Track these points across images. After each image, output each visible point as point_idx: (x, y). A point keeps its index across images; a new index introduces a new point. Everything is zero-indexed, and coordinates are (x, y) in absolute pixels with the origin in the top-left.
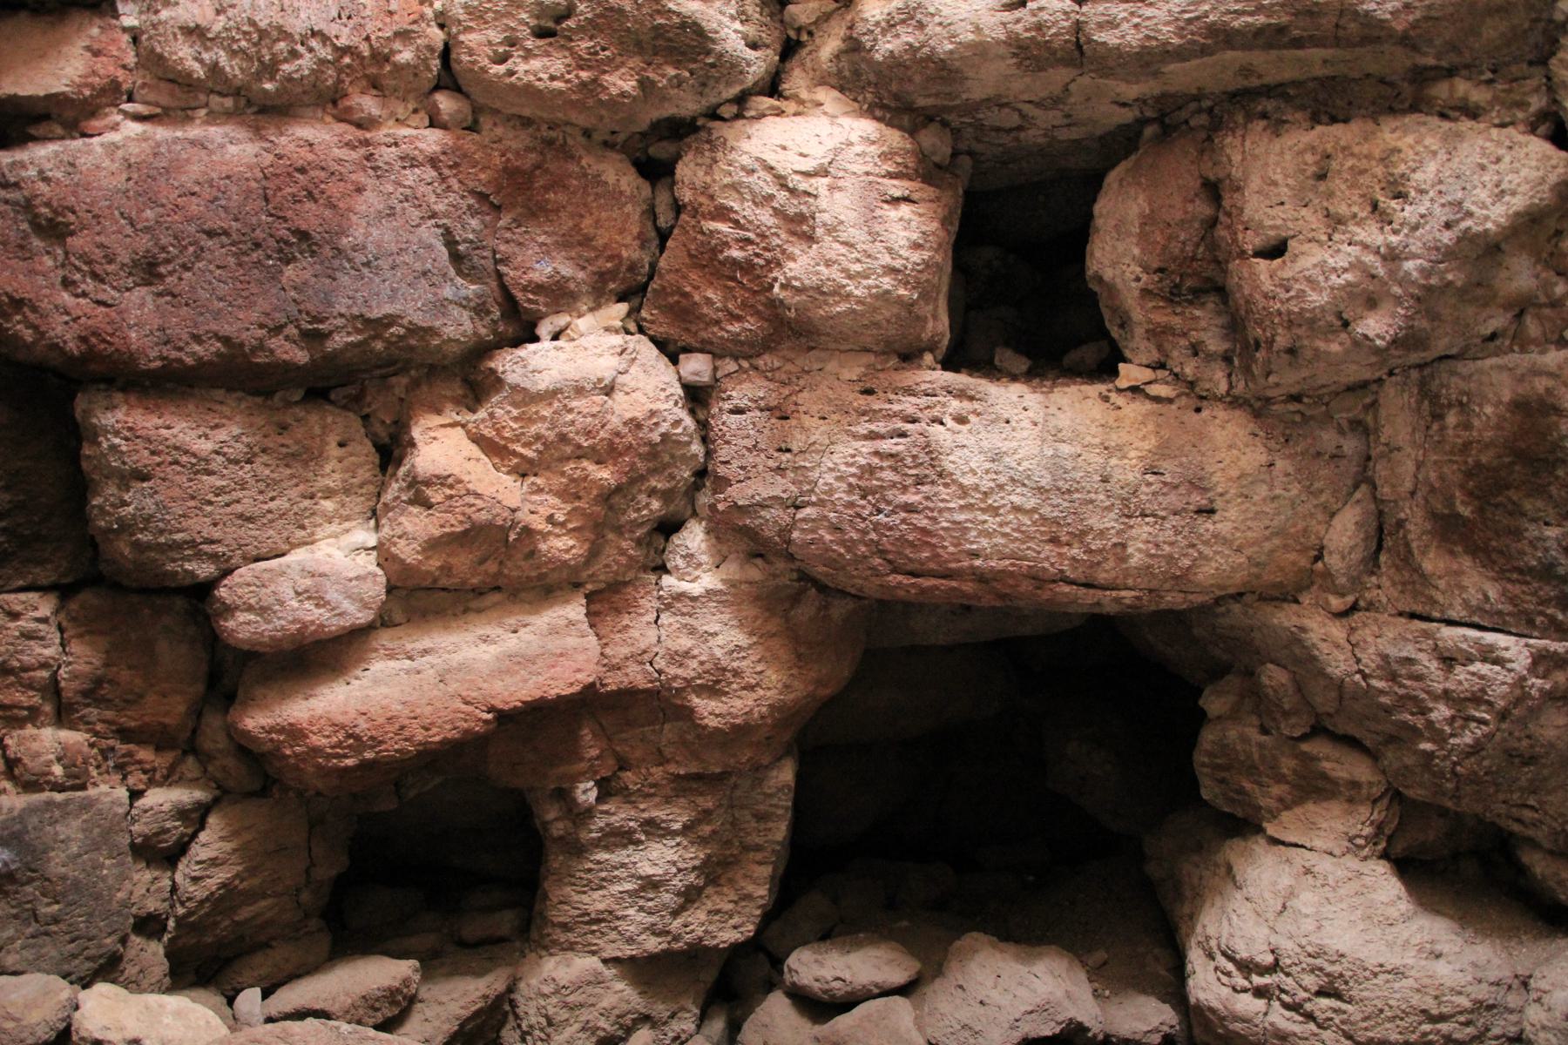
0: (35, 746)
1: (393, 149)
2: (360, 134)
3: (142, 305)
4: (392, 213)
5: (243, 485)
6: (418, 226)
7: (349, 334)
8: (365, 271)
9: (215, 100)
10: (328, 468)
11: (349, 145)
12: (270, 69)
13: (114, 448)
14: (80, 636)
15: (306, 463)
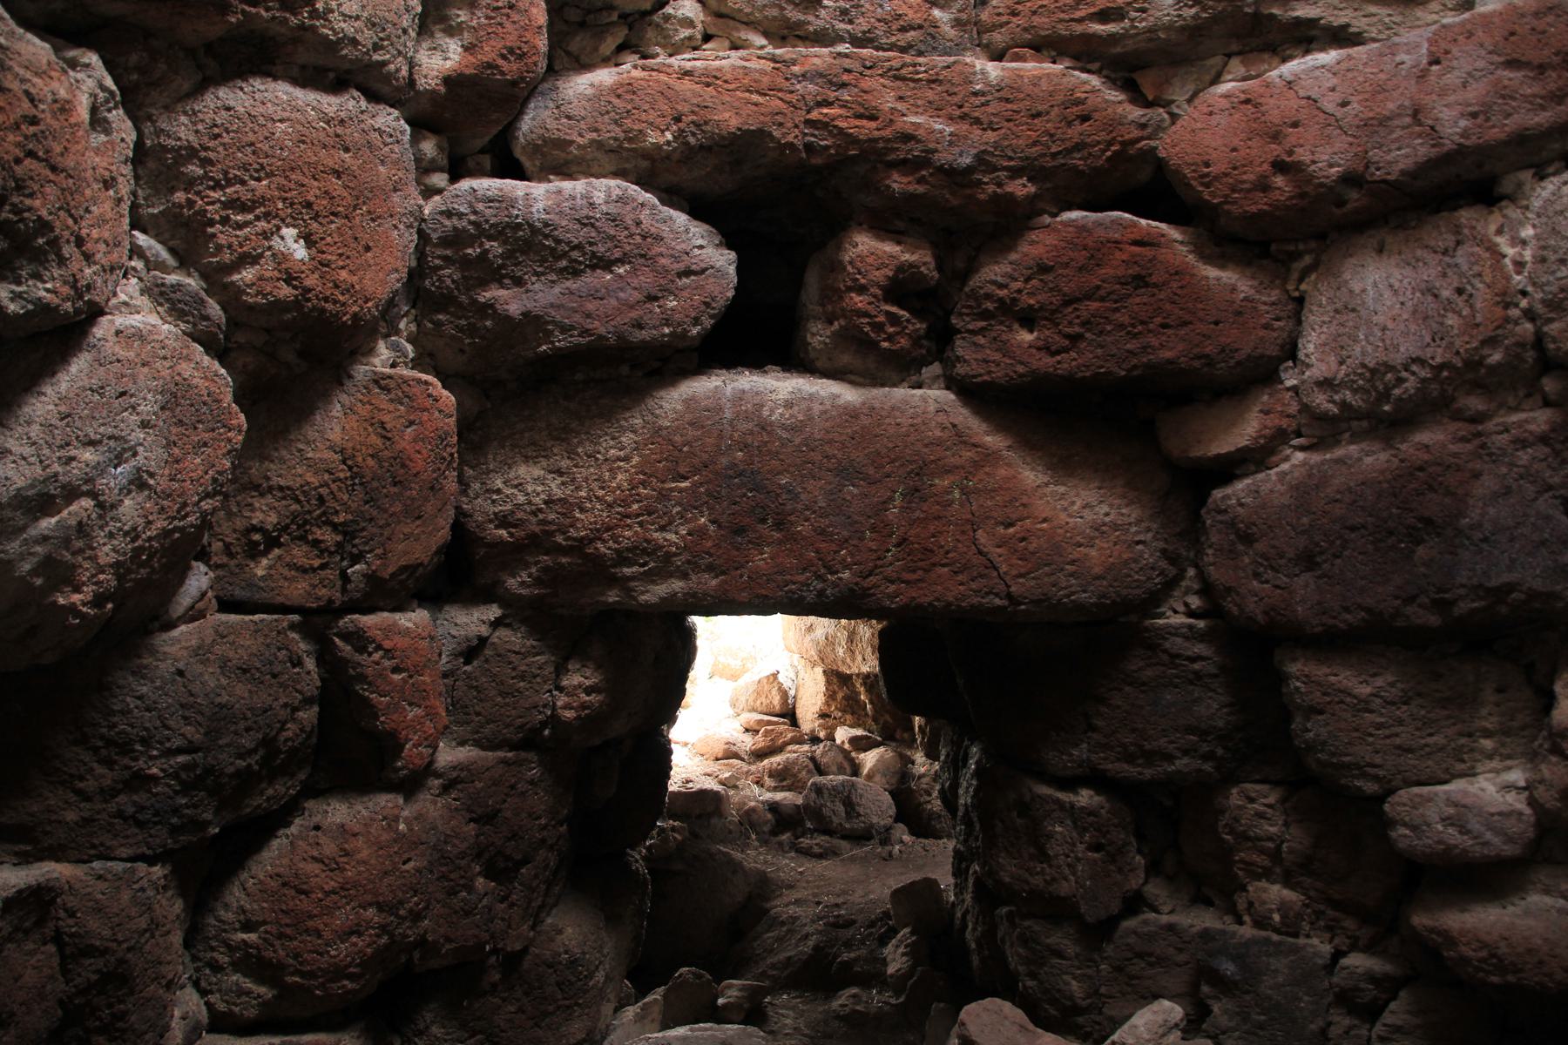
0: (1264, 896)
1: (1505, 436)
2: (1472, 428)
3: (1307, 586)
4: (1508, 491)
5: (1401, 722)
6: (1536, 499)
7: (1473, 601)
8: (1485, 546)
9: (1355, 424)
10: (1484, 712)
11: (1463, 439)
12: (1385, 396)
13: (1297, 689)
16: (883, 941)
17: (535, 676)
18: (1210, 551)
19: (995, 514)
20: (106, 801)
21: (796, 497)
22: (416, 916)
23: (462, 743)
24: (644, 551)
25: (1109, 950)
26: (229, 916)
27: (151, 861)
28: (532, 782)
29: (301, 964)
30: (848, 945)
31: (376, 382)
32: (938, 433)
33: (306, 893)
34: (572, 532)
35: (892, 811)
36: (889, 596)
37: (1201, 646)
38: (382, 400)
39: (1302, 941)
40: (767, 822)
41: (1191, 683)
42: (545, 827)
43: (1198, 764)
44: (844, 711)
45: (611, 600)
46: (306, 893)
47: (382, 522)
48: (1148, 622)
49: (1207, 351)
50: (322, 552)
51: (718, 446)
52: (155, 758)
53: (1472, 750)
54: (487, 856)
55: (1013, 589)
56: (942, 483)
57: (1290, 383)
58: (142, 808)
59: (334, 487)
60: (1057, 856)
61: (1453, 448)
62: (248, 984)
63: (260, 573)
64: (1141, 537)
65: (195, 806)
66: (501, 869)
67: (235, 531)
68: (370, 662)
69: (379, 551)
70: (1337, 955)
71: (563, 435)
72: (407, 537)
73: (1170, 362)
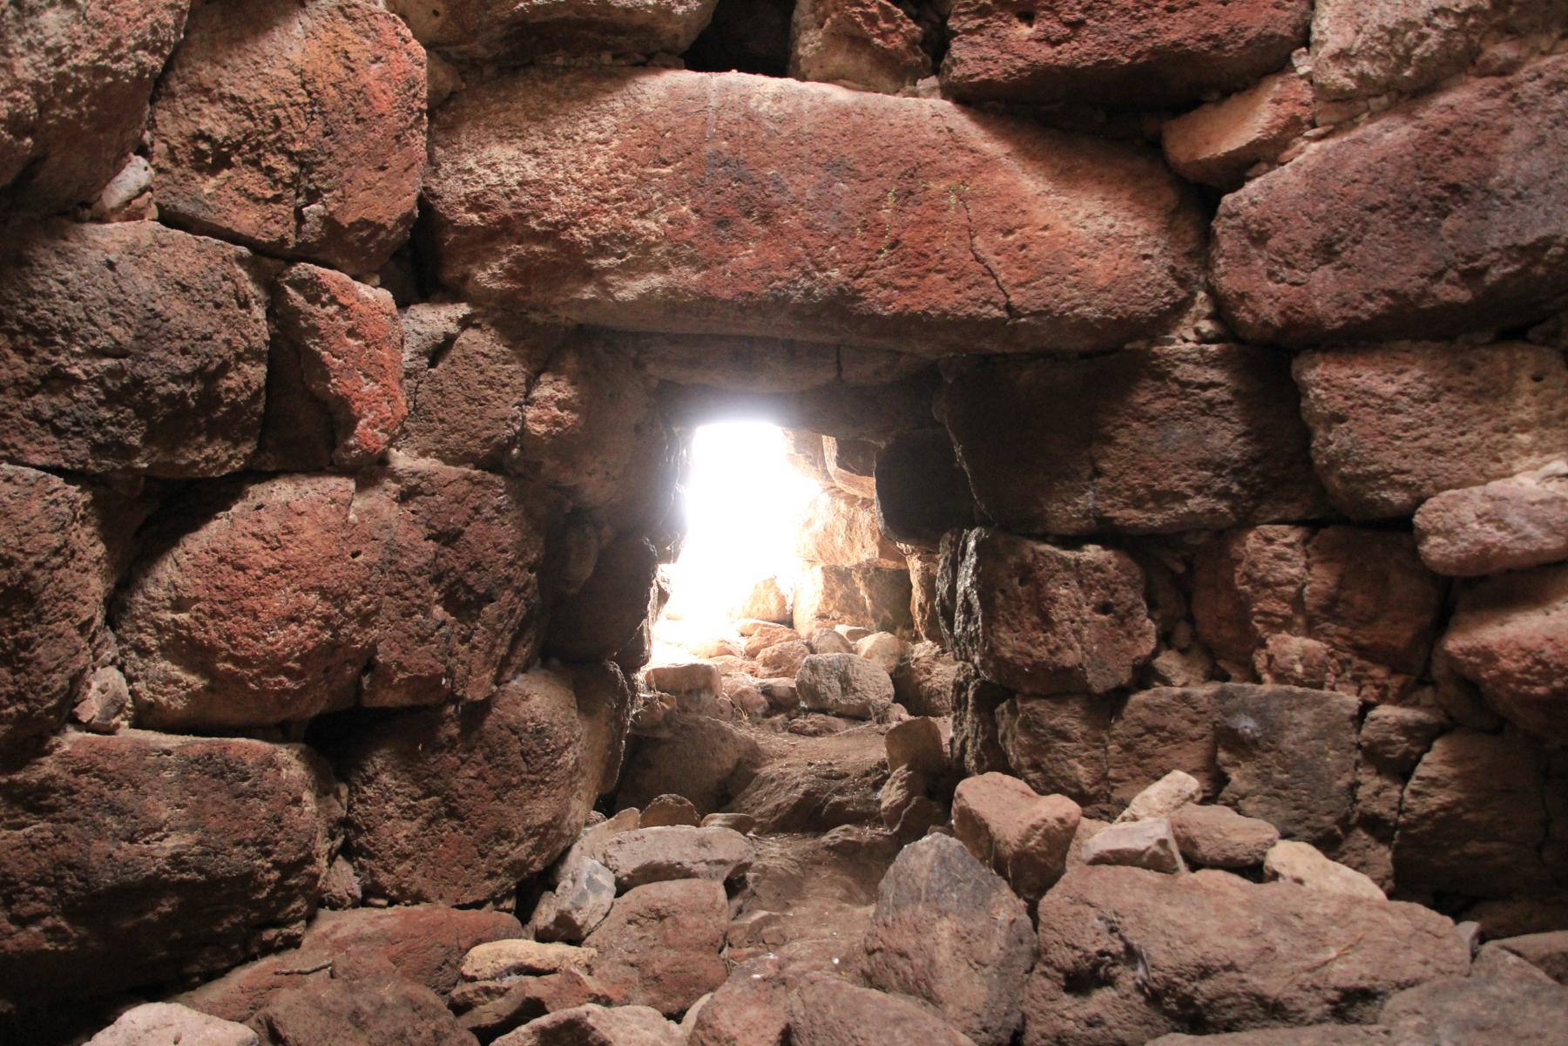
0: (1285, 647)
2: (1500, 81)
3: (1325, 278)
4: (1541, 142)
5: (1430, 421)
7: (1506, 265)
8: (1517, 203)
9: (1373, 102)
10: (1520, 402)
11: (1493, 95)
12: (1406, 59)
13: (1317, 396)
14: (1322, 562)
15: (1495, 398)
16: (877, 786)
17: (504, 386)
18: (1221, 261)
19: (993, 221)
20: (21, 398)
21: (783, 191)
22: (365, 620)
23: (424, 454)
24: (623, 241)
25: (1118, 727)
26: (158, 592)
27: (69, 476)
28: (498, 509)
29: (234, 647)
30: (840, 791)
31: (341, 9)
32: (933, 136)
33: (243, 569)
34: (547, 217)
35: (891, 690)
36: (881, 302)
37: (1214, 372)
38: (347, 29)
39: (1326, 692)
40: (759, 704)
41: (1203, 413)
42: (511, 564)
43: (1211, 503)
44: (843, 611)
45: (586, 297)
46: (243, 569)
47: (341, 160)
48: (1155, 349)
49: (1215, 31)
50: (276, 182)
51: (702, 133)
52: (78, 355)
53: (1509, 447)
54: (447, 581)
55: (1012, 299)
56: (937, 186)
57: (1302, 71)
58: (62, 414)
59: (291, 111)
60: (1061, 621)
61: (1480, 105)
62: (177, 672)
63: (206, 191)
64: (1148, 251)
65: (121, 425)
66: (463, 602)
67: (181, 134)
68: (322, 314)
69: (338, 193)
70: (1366, 707)
71: (539, 116)
72: (369, 186)
73: (1175, 44)
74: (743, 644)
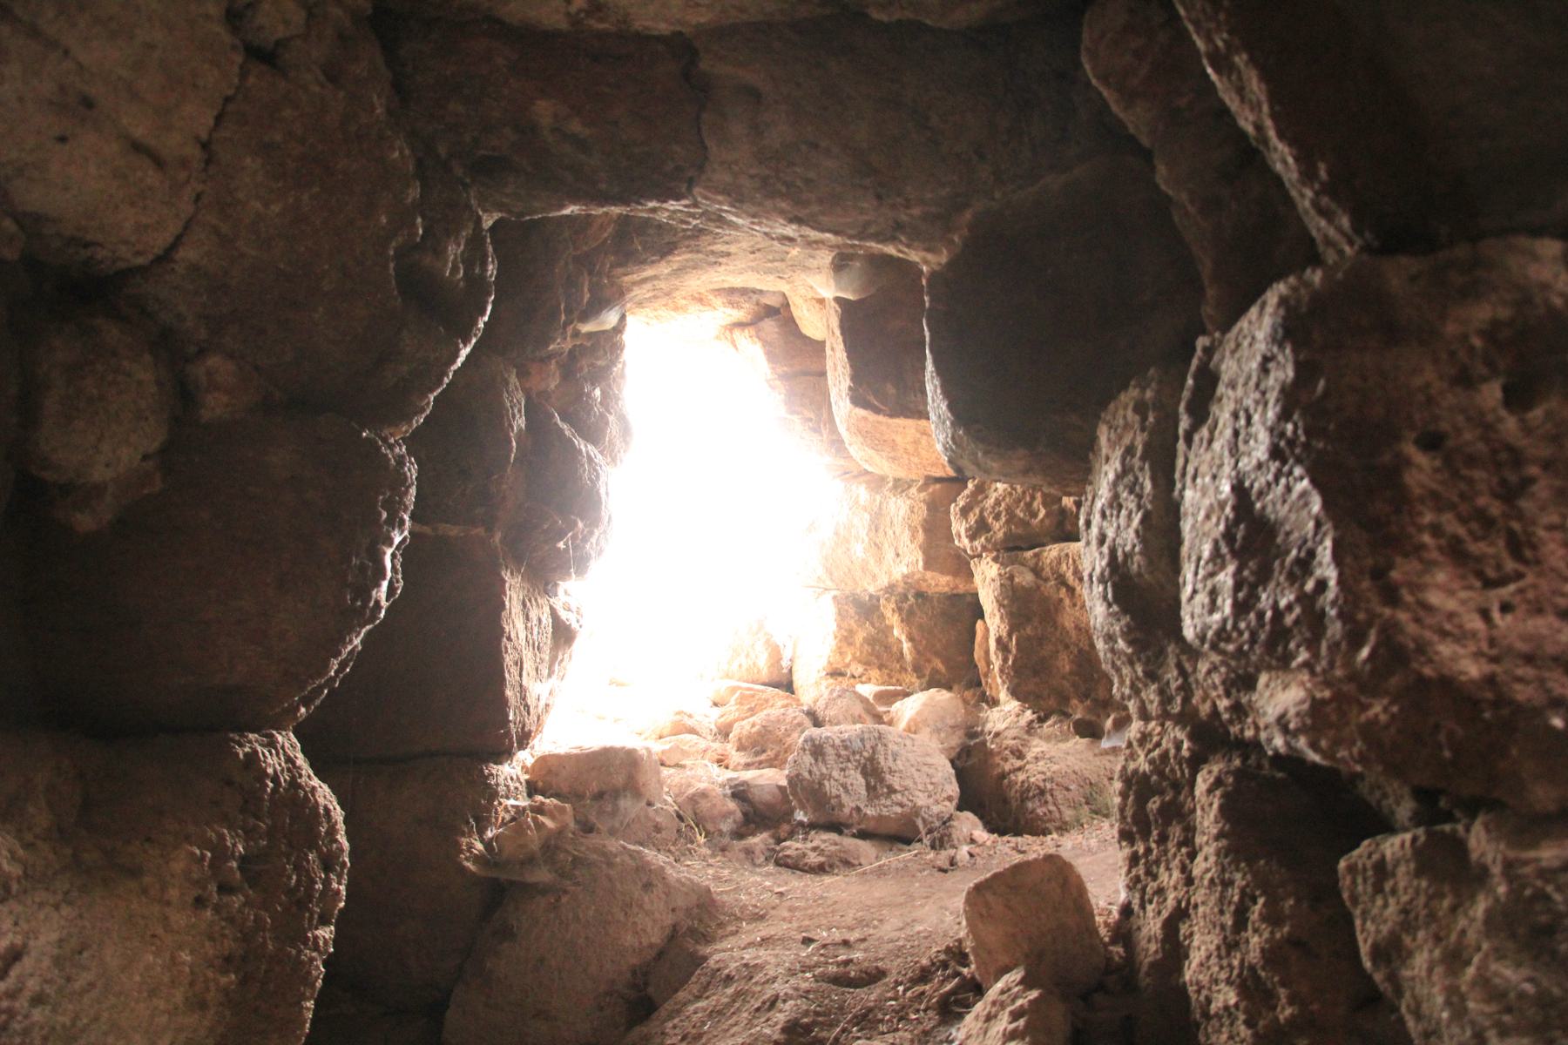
35: (953, 789)
40: (725, 815)
44: (867, 664)
74: (710, 718)
